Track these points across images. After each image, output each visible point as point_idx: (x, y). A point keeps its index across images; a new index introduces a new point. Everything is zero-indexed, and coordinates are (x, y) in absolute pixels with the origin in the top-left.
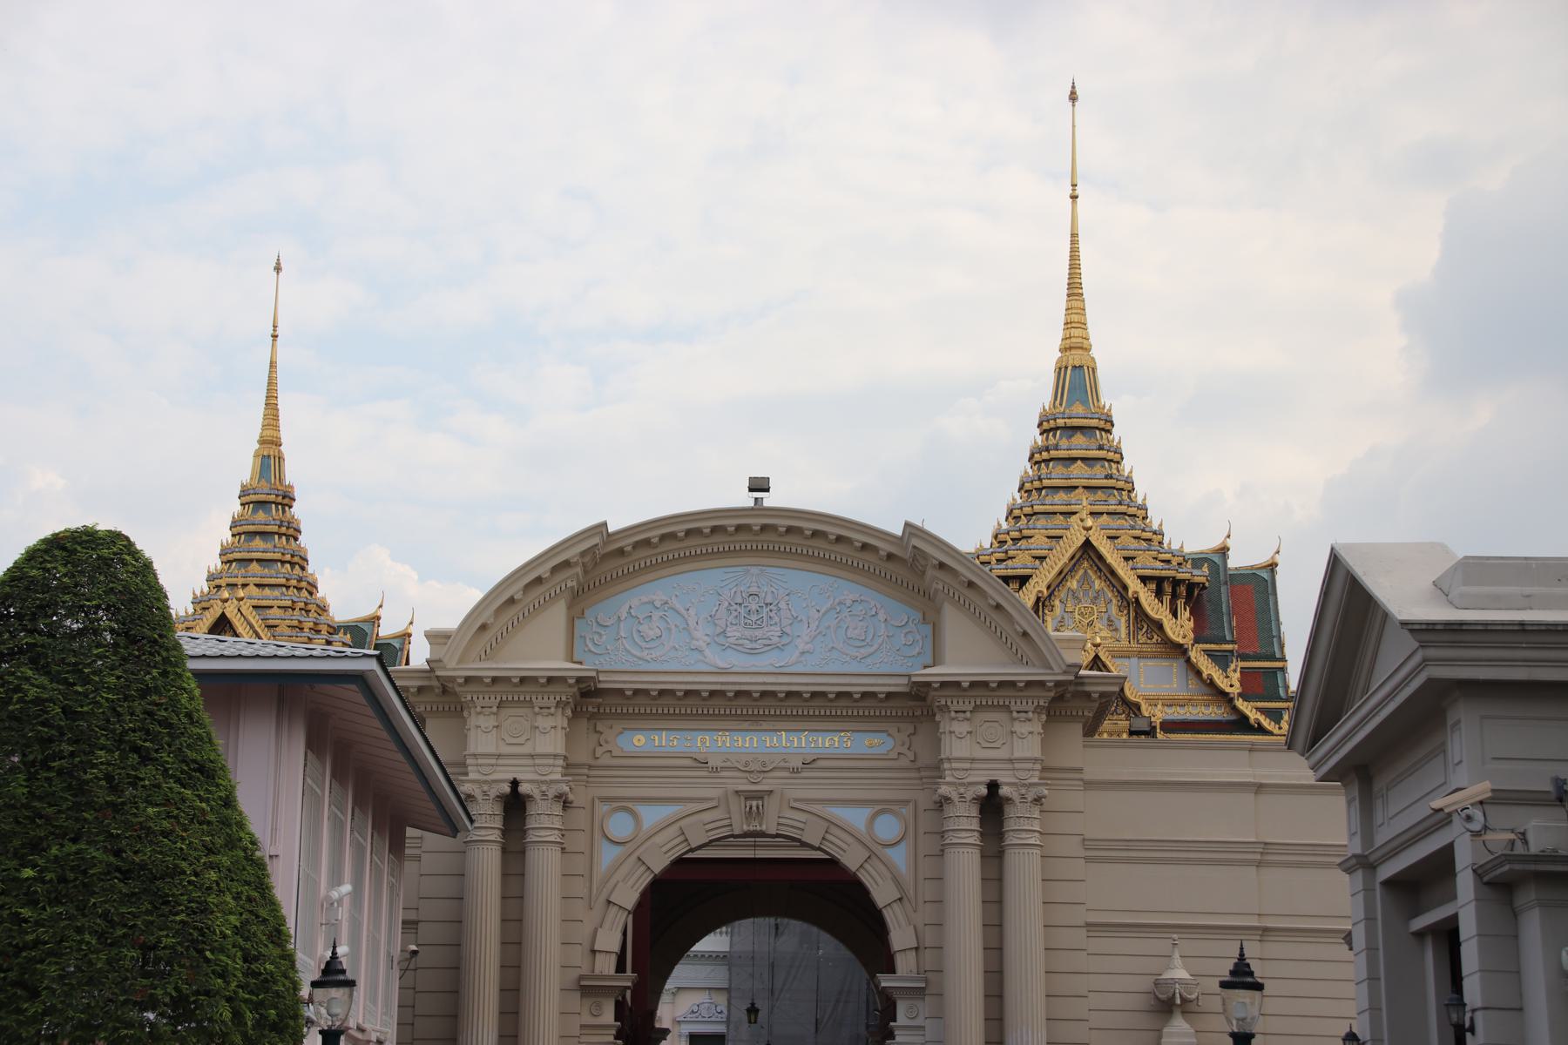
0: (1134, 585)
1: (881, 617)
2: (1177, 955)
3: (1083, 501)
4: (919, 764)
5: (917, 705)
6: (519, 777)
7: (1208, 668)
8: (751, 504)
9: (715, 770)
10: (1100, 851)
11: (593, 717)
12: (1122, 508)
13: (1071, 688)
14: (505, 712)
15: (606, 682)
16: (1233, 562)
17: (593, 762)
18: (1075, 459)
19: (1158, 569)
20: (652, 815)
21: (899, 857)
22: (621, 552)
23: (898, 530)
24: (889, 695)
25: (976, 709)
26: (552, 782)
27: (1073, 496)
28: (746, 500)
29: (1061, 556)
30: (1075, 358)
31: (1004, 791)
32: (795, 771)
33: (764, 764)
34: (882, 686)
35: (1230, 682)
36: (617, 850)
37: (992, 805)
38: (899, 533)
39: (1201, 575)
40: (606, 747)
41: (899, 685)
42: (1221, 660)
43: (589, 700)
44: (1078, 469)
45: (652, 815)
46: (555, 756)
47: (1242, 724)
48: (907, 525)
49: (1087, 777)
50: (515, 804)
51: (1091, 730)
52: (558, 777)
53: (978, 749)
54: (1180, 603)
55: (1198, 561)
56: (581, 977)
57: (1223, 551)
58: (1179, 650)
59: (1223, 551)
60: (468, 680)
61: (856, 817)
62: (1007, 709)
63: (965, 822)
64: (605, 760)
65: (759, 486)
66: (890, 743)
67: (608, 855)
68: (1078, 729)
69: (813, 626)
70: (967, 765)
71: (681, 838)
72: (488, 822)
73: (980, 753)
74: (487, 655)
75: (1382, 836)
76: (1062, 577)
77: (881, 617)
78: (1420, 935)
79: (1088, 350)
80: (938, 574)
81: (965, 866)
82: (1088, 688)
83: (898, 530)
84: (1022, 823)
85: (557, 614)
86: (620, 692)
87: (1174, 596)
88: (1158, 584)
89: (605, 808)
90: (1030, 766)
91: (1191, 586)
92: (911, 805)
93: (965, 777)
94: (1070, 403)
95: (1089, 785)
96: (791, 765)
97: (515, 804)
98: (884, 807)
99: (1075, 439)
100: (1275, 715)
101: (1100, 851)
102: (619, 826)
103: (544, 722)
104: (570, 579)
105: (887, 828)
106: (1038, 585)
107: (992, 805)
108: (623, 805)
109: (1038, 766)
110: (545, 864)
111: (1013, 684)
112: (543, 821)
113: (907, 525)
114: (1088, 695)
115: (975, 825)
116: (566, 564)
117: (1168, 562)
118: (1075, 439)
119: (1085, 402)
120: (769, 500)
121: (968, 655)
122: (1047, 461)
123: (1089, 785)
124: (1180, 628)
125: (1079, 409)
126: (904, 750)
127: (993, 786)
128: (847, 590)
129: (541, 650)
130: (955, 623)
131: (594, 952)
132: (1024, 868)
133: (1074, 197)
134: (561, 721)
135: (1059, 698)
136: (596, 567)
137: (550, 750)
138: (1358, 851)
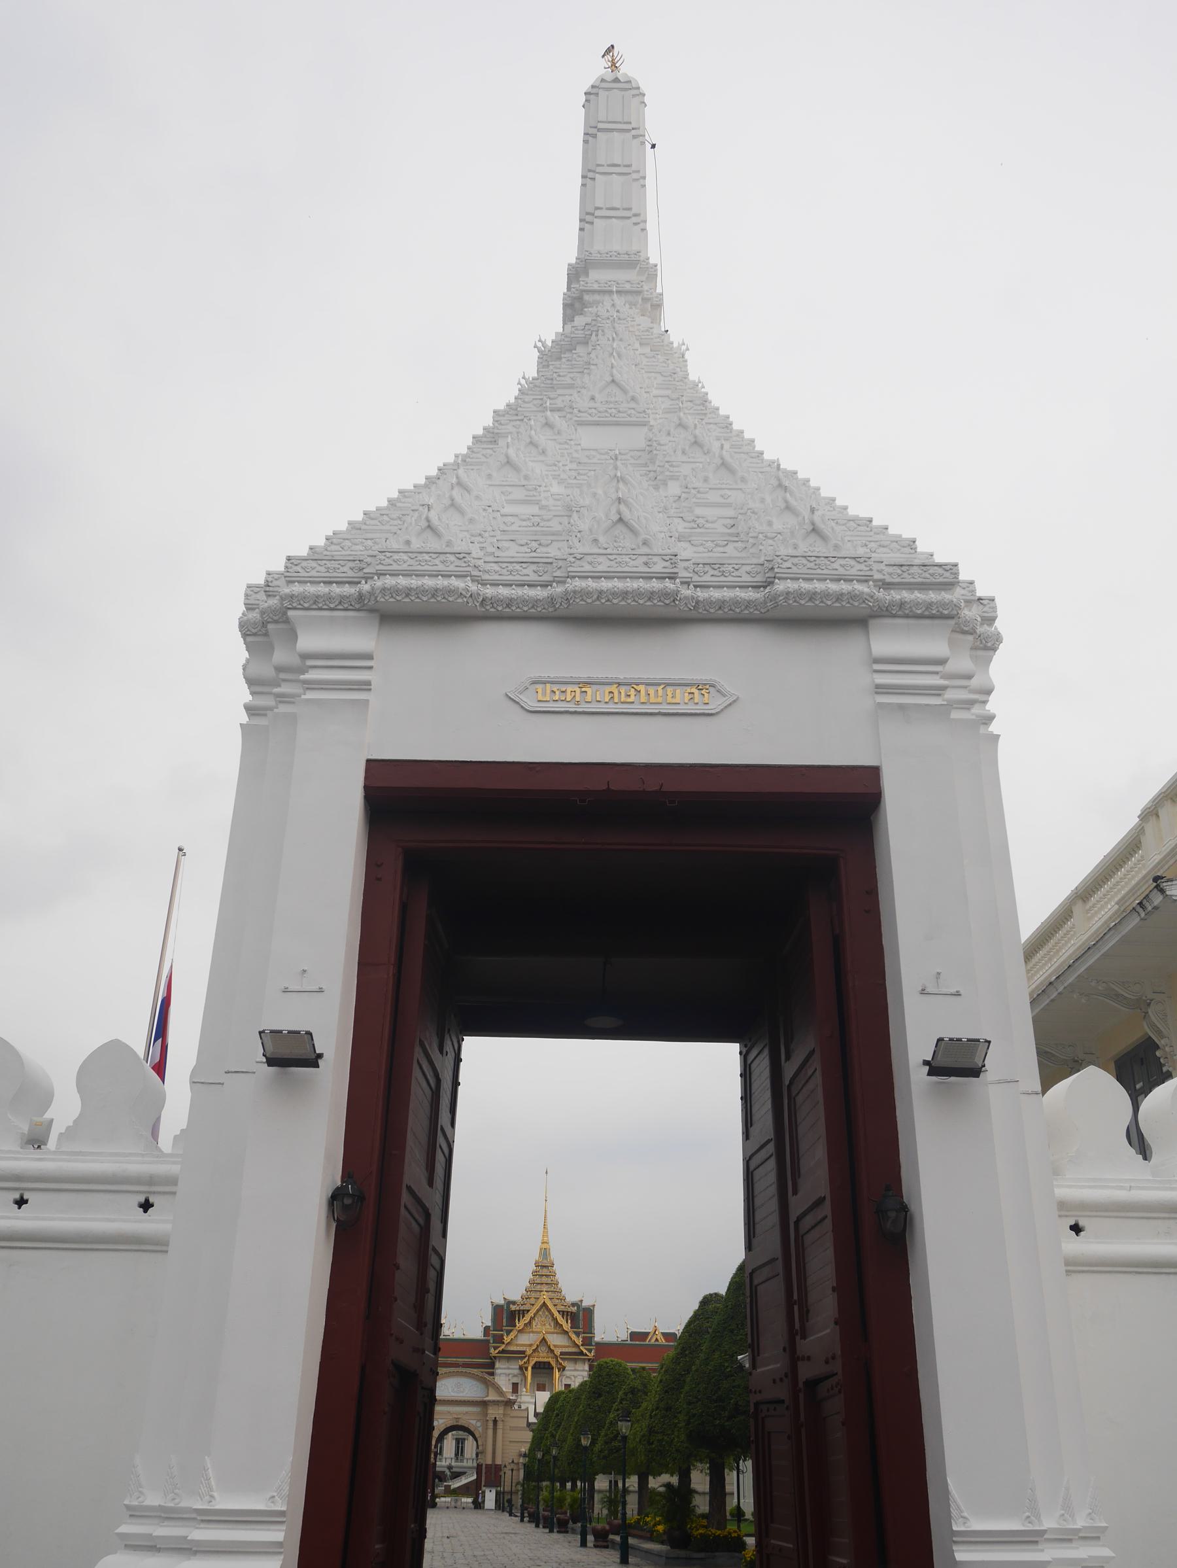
0: (556, 1314)
3: (545, 1288)
5: (484, 1404)
7: (574, 1337)
10: (513, 1429)
16: (584, 1304)
19: (562, 1308)
29: (537, 1307)
30: (545, 1246)
35: (579, 1341)
37: (495, 1421)
39: (574, 1309)
42: (578, 1334)
47: (582, 1353)
53: (493, 1412)
55: (573, 1305)
58: (566, 1333)
61: (473, 1422)
63: (491, 1424)
76: (538, 1311)
81: (490, 1432)
84: (500, 1425)
88: (562, 1313)
93: (491, 1417)
99: (544, 1270)
100: (590, 1351)
105: (479, 1424)
106: (531, 1314)
107: (495, 1421)
118: (544, 1270)
121: (493, 1396)
124: (567, 1326)
128: (474, 1382)
132: (500, 1432)
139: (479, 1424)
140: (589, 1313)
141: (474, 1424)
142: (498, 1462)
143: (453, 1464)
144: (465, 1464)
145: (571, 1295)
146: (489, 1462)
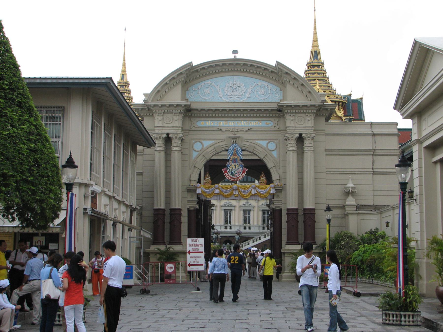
1: (269, 88)
2: (350, 180)
4: (280, 129)
5: (280, 112)
6: (169, 132)
8: (233, 57)
9: (223, 132)
10: (330, 153)
11: (190, 117)
12: (327, 85)
13: (322, 108)
14: (166, 115)
15: (193, 106)
16: (353, 97)
17: (189, 129)
18: (315, 73)
20: (206, 144)
21: (275, 154)
22: (197, 71)
23: (274, 64)
24: (272, 110)
25: (296, 113)
26: (178, 134)
27: (314, 82)
28: (232, 56)
31: (303, 135)
32: (246, 131)
33: (237, 130)
34: (270, 107)
36: (197, 153)
37: (300, 139)
38: (274, 65)
40: (193, 125)
41: (275, 106)
43: (188, 112)
44: (316, 75)
45: (206, 144)
46: (179, 127)
48: (277, 62)
49: (327, 132)
50: (168, 140)
51: (328, 119)
52: (180, 132)
54: (340, 107)
55: (344, 97)
56: (188, 187)
57: (350, 95)
59: (350, 95)
60: (154, 106)
62: (305, 113)
63: (292, 145)
64: (193, 129)
65: (235, 52)
66: (272, 124)
67: (195, 154)
68: (324, 119)
69: (250, 90)
70: (294, 128)
71: (214, 150)
72: (160, 144)
73: (297, 125)
74: (160, 100)
75: (424, 134)
77: (269, 88)
78: (435, 163)
79: (318, 47)
80: (286, 75)
82: (326, 108)
83: (274, 64)
84: (308, 144)
85: (179, 87)
86: (197, 110)
87: (339, 105)
89: (193, 142)
90: (311, 128)
91: (343, 103)
92: (278, 140)
94: (314, 59)
95: (327, 134)
96: (244, 130)
97: (168, 140)
98: (271, 140)
101: (330, 153)
102: (197, 146)
103: (176, 118)
104: (182, 78)
107: (300, 139)
108: (198, 140)
109: (313, 129)
110: (176, 156)
111: (306, 106)
112: (176, 144)
113: (277, 62)
114: (327, 109)
115: (295, 145)
116: (181, 73)
117: (337, 97)
119: (317, 59)
120: (239, 56)
121: (294, 97)
122: (308, 74)
123: (327, 134)
125: (316, 61)
126: (276, 125)
127: (301, 134)
129: (175, 97)
130: (290, 90)
131: (191, 180)
132: (308, 157)
133: (315, 10)
134: (180, 117)
135: (319, 110)
136: (189, 75)
137: (178, 126)
138: (417, 138)
139: (272, 146)
140: (358, 104)
141: (267, 148)
142: (309, 204)
143: (242, 230)
144: (252, 230)
145: (341, 88)
146: (292, 204)
